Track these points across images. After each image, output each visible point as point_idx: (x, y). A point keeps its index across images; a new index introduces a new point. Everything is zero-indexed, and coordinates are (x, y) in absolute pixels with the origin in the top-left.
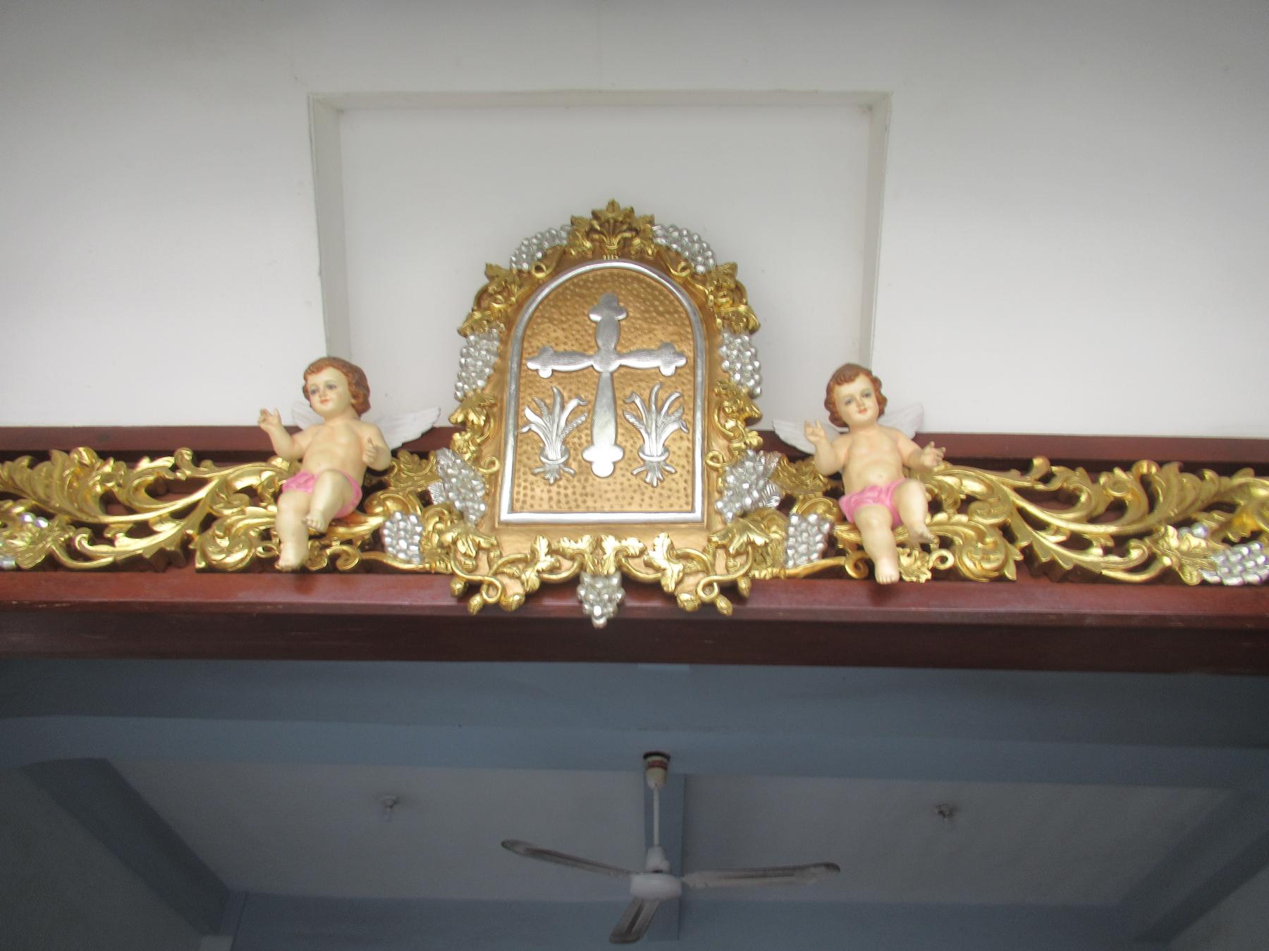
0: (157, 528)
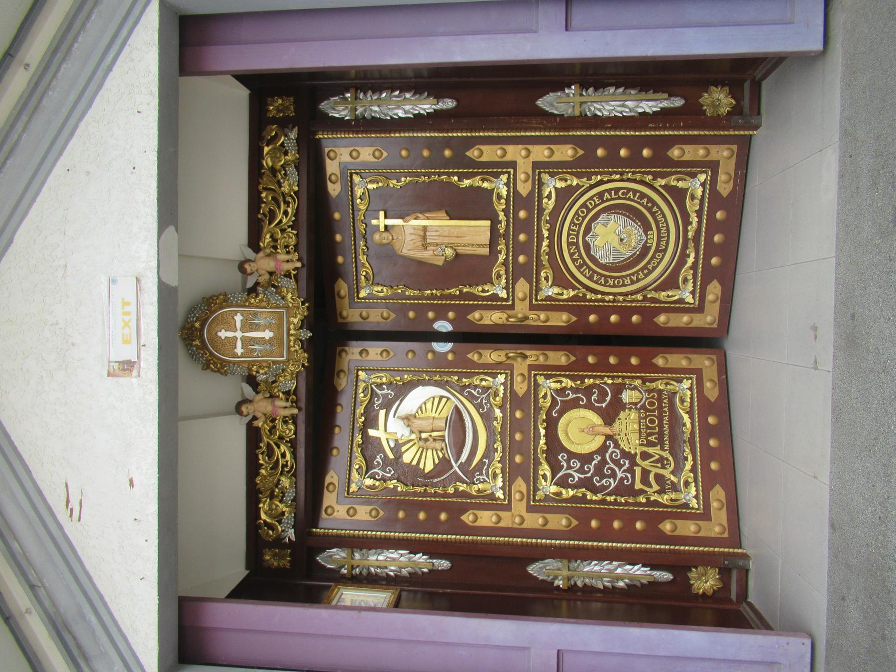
0: (283, 451)
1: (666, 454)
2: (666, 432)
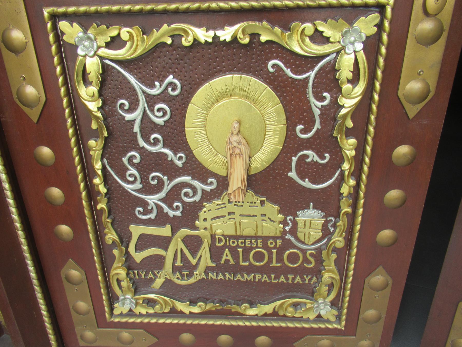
1: (199, 274)
2: (239, 277)
